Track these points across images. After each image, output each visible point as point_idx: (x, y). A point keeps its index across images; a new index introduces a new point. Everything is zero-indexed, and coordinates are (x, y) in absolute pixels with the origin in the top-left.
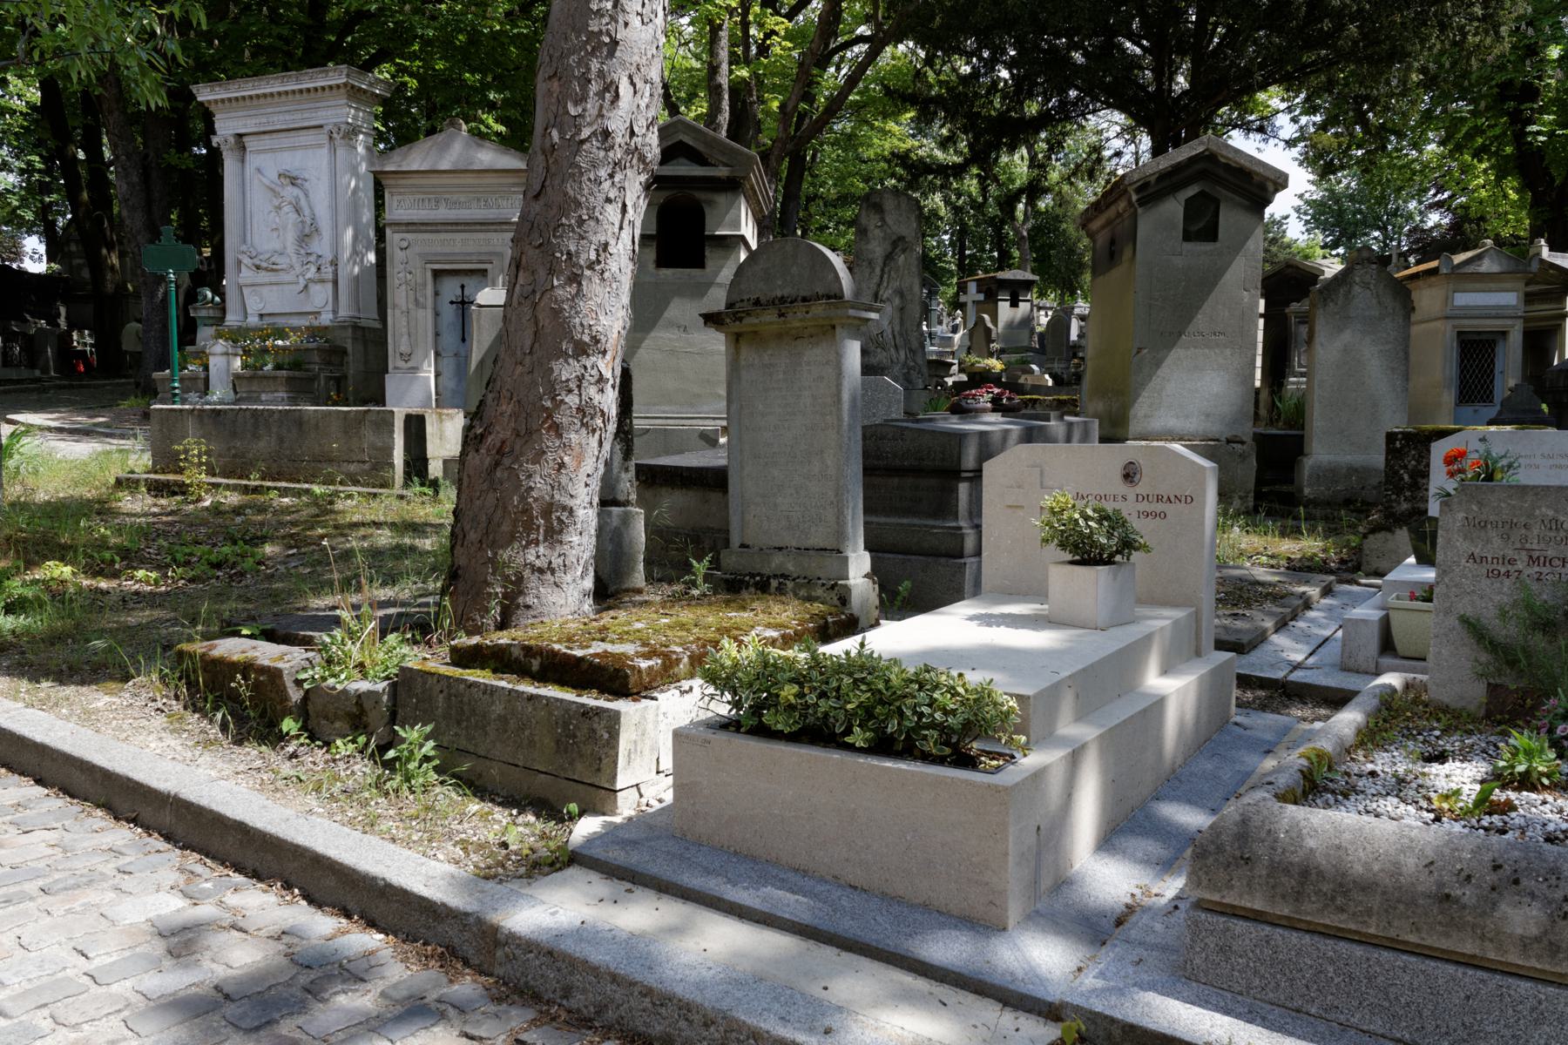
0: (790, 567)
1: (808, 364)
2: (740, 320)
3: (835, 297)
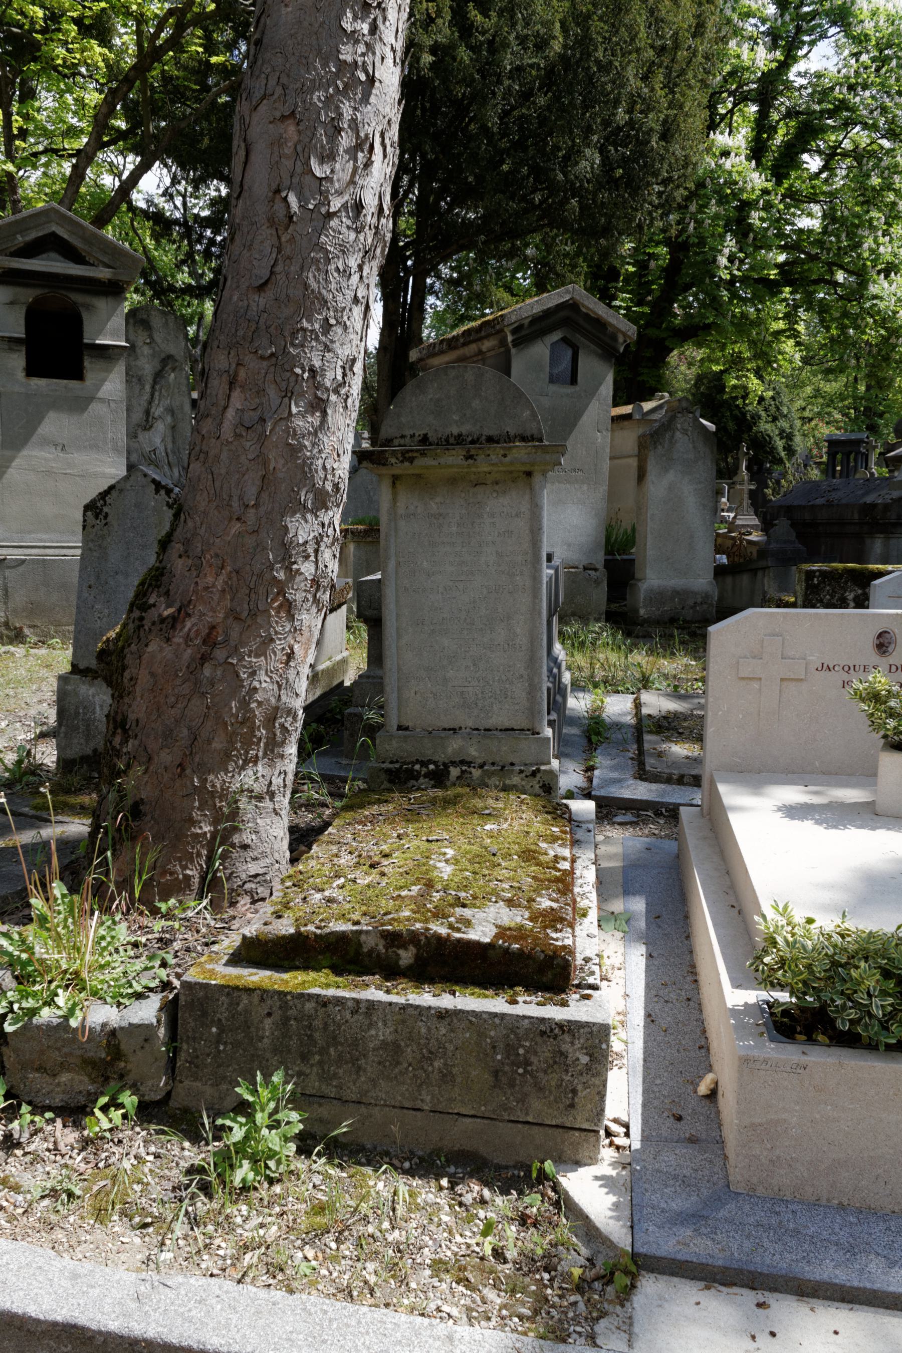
0: (473, 752)
1: (492, 515)
2: (411, 460)
3: (532, 438)
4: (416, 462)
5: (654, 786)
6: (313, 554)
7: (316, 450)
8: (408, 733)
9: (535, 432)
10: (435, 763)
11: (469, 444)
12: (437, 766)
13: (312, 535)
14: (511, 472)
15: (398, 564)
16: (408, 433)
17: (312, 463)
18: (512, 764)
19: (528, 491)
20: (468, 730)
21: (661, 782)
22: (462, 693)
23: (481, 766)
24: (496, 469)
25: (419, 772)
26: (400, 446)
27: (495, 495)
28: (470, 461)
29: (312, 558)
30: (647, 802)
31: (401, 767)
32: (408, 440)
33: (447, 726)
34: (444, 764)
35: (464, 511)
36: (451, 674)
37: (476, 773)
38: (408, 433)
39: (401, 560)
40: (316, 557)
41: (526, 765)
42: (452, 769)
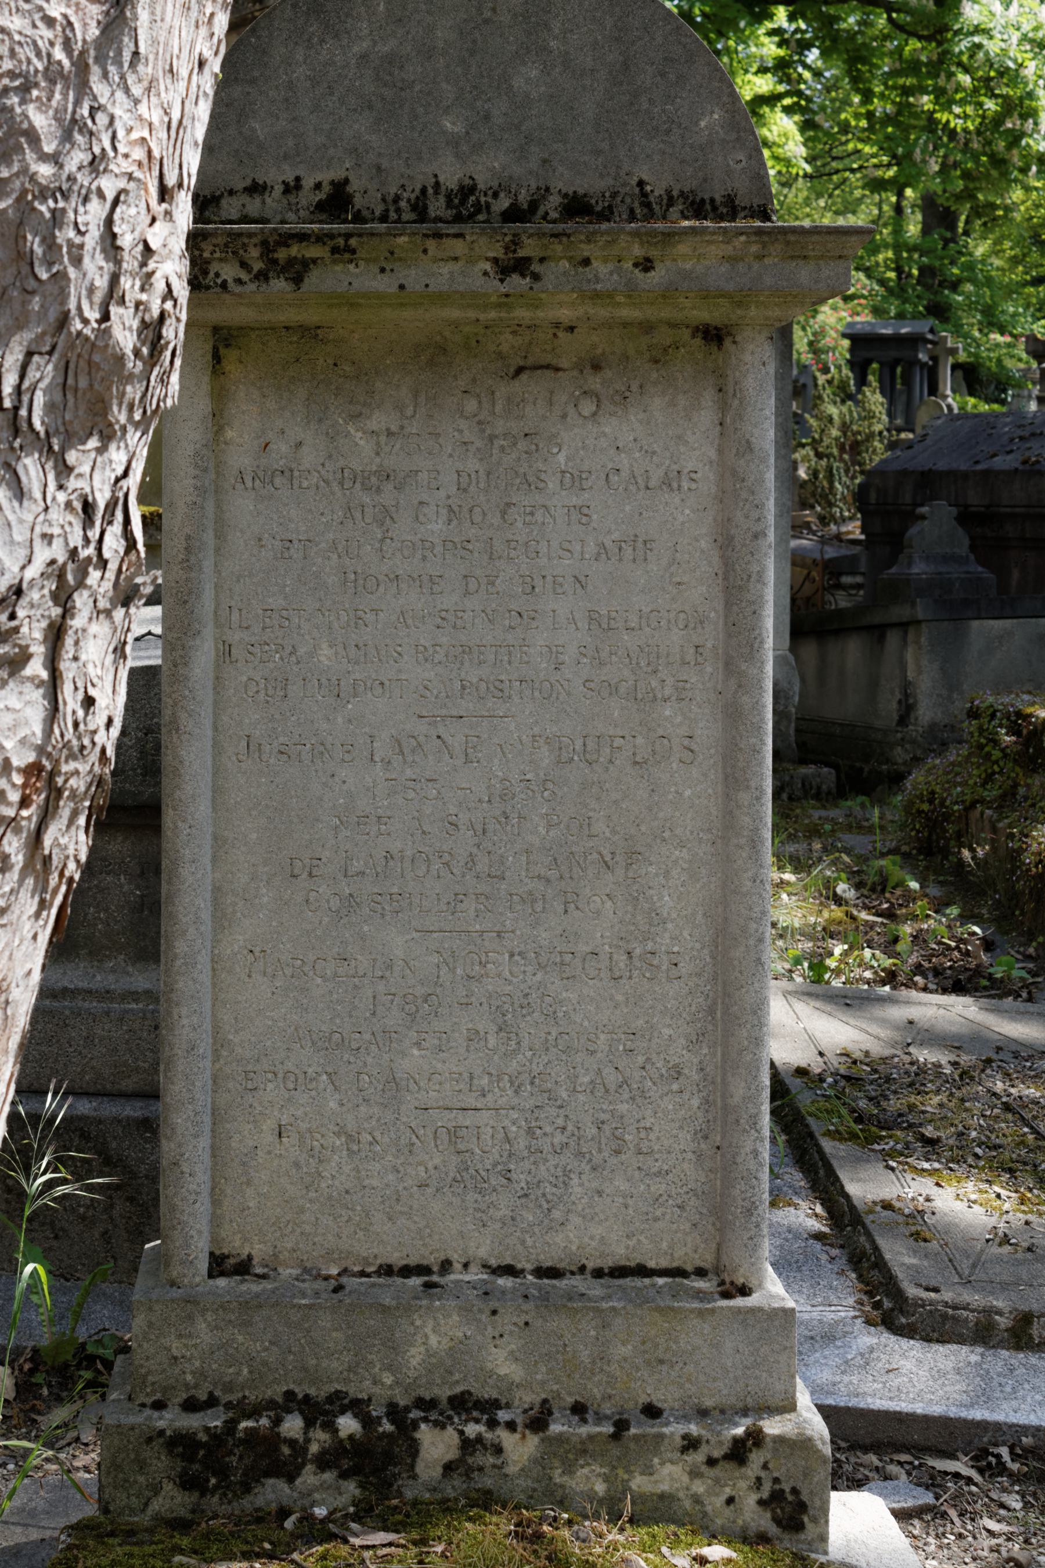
0: (504, 1364)
1: (576, 480)
2: (297, 272)
3: (730, 208)
4: (313, 280)
5: (948, 1357)
6: (38, 650)
7: (76, 159)
8: (254, 1287)
9: (741, 187)
10: (357, 1407)
11: (524, 224)
12: (368, 1422)
13: (42, 555)
14: (647, 327)
15: (226, 652)
16: (275, 175)
17: (57, 217)
18: (652, 1412)
19: (709, 398)
20: (476, 1275)
21: (961, 1341)
22: (454, 1133)
23: (538, 1423)
24: (602, 313)
25: (299, 1448)
26: (245, 219)
27: (588, 407)
28: (517, 283)
29: (36, 668)
30: (944, 1422)
31: (231, 1425)
32: (273, 201)
33: (397, 1259)
34: (394, 1412)
35: (472, 464)
36: (413, 1060)
37: (520, 1449)
38: (275, 175)
39: (235, 637)
40: (52, 663)
41: (703, 1413)
42: (425, 1433)
